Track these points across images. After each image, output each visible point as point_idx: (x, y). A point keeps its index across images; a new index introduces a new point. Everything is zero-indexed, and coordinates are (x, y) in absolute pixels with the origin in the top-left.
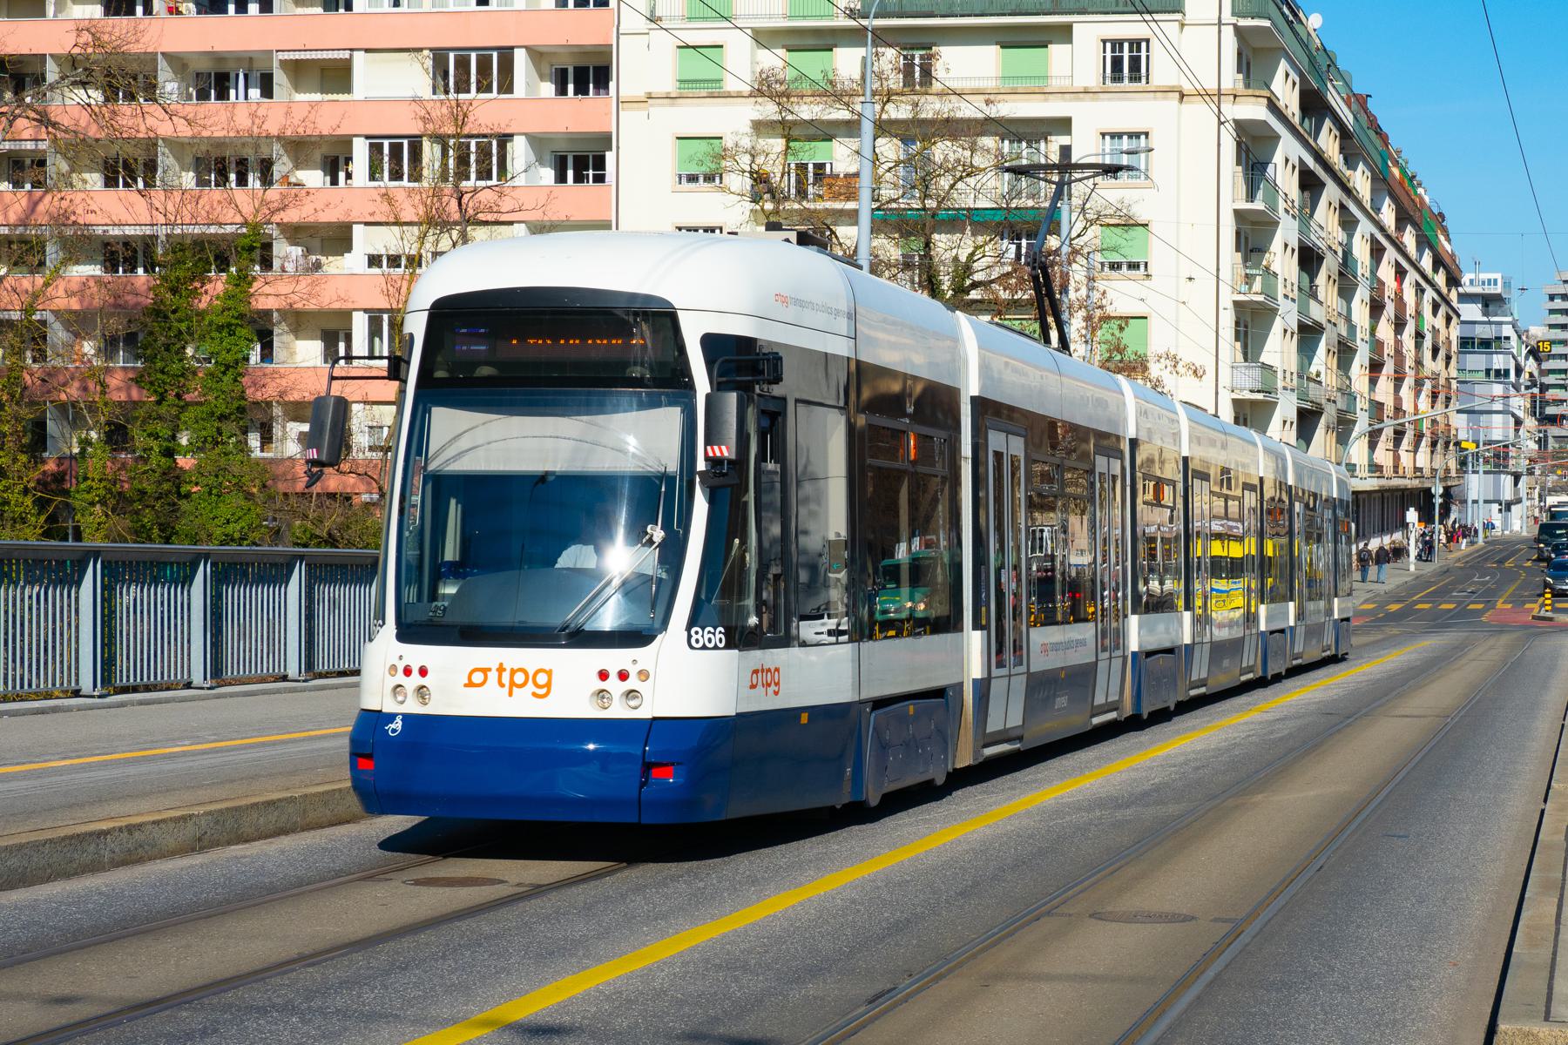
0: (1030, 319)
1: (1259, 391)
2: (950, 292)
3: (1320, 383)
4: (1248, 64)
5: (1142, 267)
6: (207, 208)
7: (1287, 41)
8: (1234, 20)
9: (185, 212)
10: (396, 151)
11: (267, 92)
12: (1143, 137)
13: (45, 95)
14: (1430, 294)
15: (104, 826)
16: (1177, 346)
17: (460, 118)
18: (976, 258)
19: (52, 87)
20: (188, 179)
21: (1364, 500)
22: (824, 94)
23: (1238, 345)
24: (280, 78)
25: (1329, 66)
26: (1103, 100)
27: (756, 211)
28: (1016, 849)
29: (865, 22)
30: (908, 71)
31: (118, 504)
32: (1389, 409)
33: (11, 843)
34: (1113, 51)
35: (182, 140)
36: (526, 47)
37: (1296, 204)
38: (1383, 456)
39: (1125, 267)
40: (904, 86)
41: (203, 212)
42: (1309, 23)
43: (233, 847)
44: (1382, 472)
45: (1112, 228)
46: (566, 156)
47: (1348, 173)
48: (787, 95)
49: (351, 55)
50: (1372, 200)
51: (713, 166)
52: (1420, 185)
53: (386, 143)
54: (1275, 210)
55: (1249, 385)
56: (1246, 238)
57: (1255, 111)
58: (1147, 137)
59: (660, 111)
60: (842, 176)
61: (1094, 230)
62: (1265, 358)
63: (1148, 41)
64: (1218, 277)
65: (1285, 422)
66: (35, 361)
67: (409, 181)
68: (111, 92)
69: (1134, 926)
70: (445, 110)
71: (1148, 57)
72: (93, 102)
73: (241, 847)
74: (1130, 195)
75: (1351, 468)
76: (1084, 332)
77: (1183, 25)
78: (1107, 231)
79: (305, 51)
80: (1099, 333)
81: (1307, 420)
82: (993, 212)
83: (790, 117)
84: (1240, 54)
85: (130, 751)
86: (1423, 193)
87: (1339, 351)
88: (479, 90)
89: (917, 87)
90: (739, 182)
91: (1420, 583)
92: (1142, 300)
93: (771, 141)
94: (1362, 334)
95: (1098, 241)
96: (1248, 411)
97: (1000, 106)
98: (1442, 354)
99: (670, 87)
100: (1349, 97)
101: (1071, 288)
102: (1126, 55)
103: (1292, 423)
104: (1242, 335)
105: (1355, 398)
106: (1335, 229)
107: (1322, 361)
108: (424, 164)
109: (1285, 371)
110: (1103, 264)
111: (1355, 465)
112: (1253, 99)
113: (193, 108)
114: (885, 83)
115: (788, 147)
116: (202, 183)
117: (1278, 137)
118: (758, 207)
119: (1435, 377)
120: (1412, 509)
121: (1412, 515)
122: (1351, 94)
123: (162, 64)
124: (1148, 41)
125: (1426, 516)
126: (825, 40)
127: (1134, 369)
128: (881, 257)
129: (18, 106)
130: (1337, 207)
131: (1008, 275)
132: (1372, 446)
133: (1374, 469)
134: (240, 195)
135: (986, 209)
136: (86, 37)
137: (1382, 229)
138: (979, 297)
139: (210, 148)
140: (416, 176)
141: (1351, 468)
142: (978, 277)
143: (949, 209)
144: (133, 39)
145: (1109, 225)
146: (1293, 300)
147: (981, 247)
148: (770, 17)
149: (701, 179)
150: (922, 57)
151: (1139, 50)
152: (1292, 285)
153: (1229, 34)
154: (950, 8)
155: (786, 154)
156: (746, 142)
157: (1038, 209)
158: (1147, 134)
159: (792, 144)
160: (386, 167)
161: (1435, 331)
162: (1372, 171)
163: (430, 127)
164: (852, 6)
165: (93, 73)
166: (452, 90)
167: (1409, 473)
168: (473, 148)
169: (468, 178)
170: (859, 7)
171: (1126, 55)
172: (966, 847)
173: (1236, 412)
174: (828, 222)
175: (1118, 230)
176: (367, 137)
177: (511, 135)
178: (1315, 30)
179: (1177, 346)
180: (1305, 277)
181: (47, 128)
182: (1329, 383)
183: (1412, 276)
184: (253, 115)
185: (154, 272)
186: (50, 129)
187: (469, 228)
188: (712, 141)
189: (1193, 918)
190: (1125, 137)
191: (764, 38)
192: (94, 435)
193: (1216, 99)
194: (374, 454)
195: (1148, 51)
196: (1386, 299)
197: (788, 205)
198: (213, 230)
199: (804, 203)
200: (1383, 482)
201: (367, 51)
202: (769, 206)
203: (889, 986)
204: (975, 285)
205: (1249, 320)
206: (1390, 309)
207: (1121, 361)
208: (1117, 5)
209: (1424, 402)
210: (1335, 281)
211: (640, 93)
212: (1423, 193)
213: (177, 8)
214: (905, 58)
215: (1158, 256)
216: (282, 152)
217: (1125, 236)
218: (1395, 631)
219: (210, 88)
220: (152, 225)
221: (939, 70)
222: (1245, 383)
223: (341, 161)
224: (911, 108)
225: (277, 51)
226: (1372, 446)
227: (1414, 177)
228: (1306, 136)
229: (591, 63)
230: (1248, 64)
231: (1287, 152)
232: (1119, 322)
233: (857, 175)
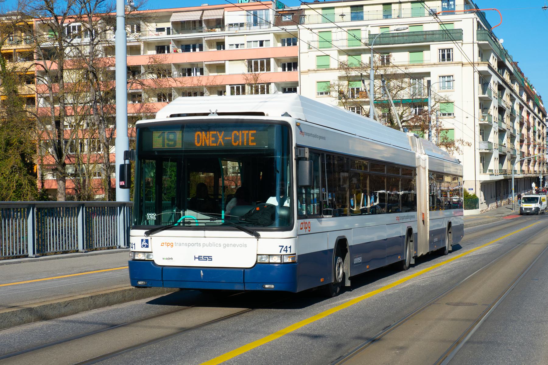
8: (477, 42)
30: (382, 60)
39: (447, 115)
59: (312, 75)
74: (448, 94)
97: (409, 69)
99: (315, 67)
126: (358, 52)
153: (476, 46)
156: (337, 83)
175: (445, 104)
191: (341, 52)
197: (349, 100)
202: (344, 101)
211: (306, 70)
222: (483, 147)
231: (494, 79)
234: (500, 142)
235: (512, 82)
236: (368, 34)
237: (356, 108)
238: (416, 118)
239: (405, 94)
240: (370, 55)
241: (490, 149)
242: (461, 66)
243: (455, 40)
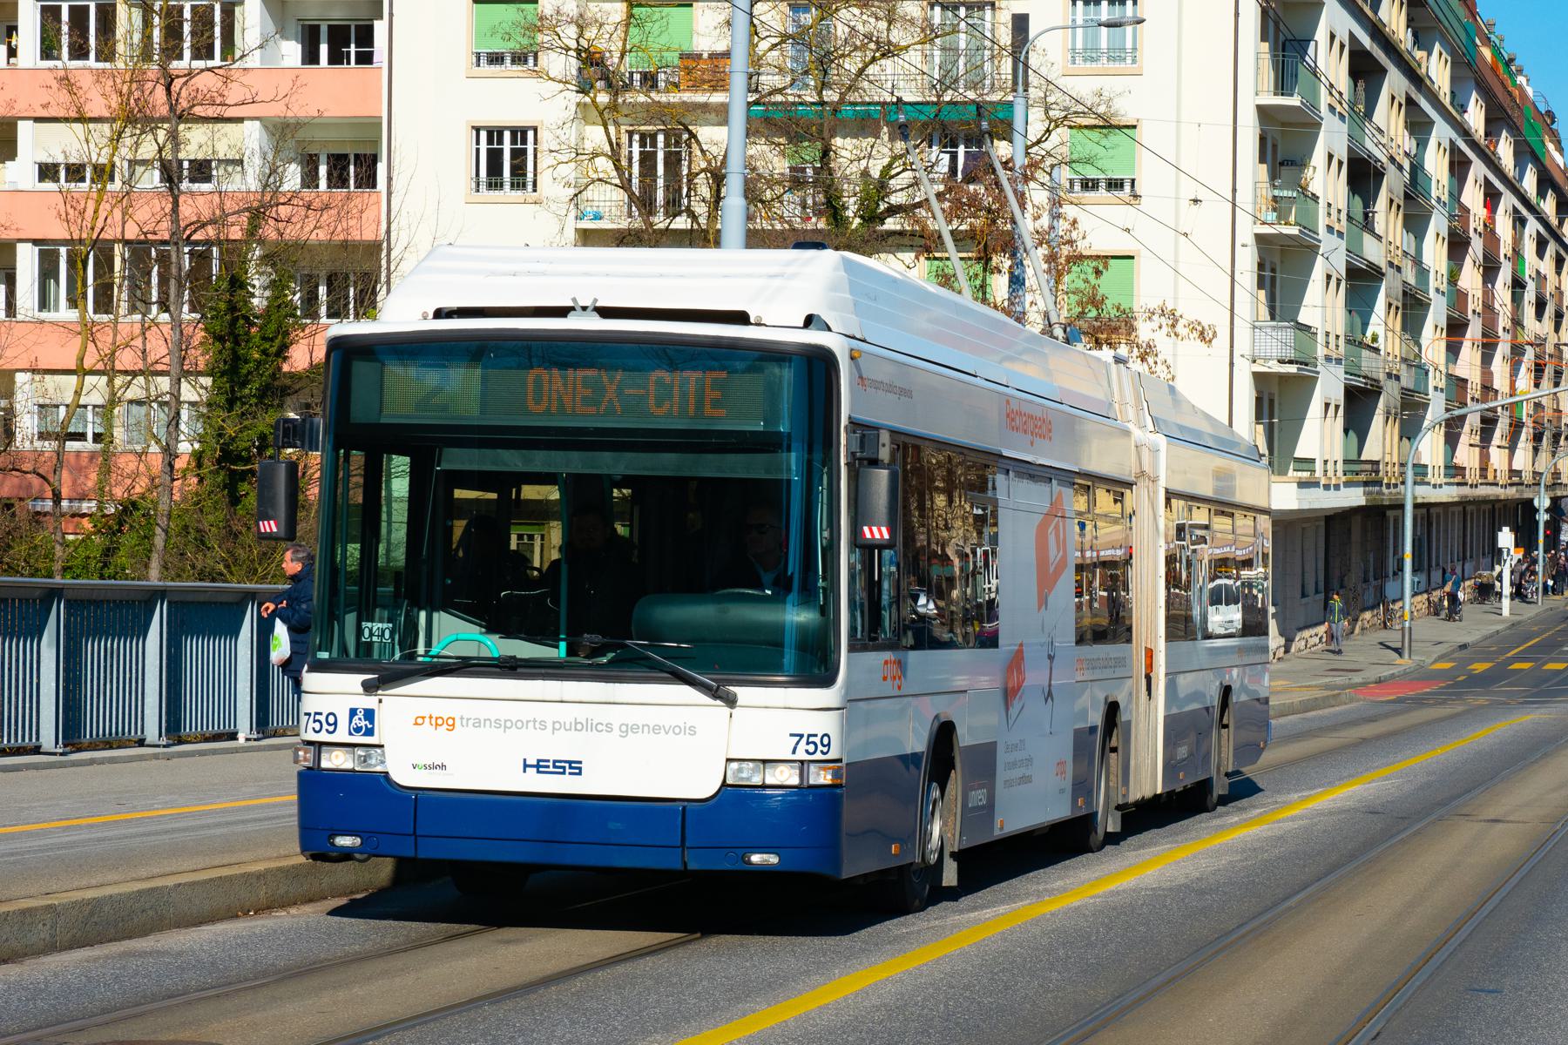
0: (970, 259)
1: (1291, 362)
2: (858, 221)
3: (1377, 350)
5: (1127, 187)
14: (1533, 226)
16: (1176, 298)
18: (893, 172)
21: (1438, 516)
23: (1262, 294)
27: (585, 104)
28: (946, 1006)
32: (1474, 388)
37: (1346, 96)
38: (1466, 455)
44: (1464, 477)
46: (319, 26)
50: (1452, 92)
51: (525, 41)
52: (1520, 71)
54: (1315, 107)
56: (1275, 146)
60: (705, 56)
61: (1060, 134)
62: (1304, 317)
64: (1234, 205)
65: (1327, 405)
67: (97, 60)
74: (1110, 85)
75: (1421, 470)
78: (1079, 135)
80: (1066, 279)
86: (1524, 83)
87: (1405, 306)
90: (560, 64)
91: (1517, 633)
92: (1128, 230)
94: (1437, 281)
95: (1065, 150)
96: (1275, 390)
98: (1550, 310)
103: (1337, 407)
105: (1427, 373)
107: (1382, 322)
108: (118, 36)
109: (1327, 334)
110: (1071, 182)
111: (1426, 466)
115: (631, 16)
118: (587, 100)
119: (1539, 343)
120: (1506, 529)
121: (1506, 538)
125: (1526, 539)
127: (1116, 330)
128: (761, 171)
130: (1403, 102)
132: (1452, 440)
133: (1452, 471)
137: (1465, 132)
138: (898, 227)
140: (106, 54)
141: (1419, 470)
142: (897, 199)
143: (854, 104)
145: (1081, 127)
146: (1340, 234)
147: (901, 156)
149: (508, 60)
152: (1339, 211)
155: (628, 25)
159: (636, 11)
160: (65, 40)
161: (1540, 278)
162: (1453, 53)
167: (1503, 478)
169: (180, 57)
172: (875, 1001)
173: (1258, 391)
174: (686, 121)
175: (1095, 135)
179: (1176, 298)
180: (1358, 200)
182: (1390, 350)
183: (1508, 201)
187: (181, 127)
194: (46, 443)
196: (1472, 233)
197: (629, 97)
199: (653, 95)
200: (1466, 491)
202: (603, 98)
204: (893, 210)
205: (1277, 260)
206: (1477, 246)
207: (1096, 319)
209: (1524, 381)
210: (1399, 207)
212: (1524, 83)
215: (1149, 175)
217: (1105, 141)
218: (1482, 700)
226: (1452, 440)
227: (1512, 60)
232: (1095, 264)
233: (727, 55)
234: (1350, 327)
237: (661, 138)
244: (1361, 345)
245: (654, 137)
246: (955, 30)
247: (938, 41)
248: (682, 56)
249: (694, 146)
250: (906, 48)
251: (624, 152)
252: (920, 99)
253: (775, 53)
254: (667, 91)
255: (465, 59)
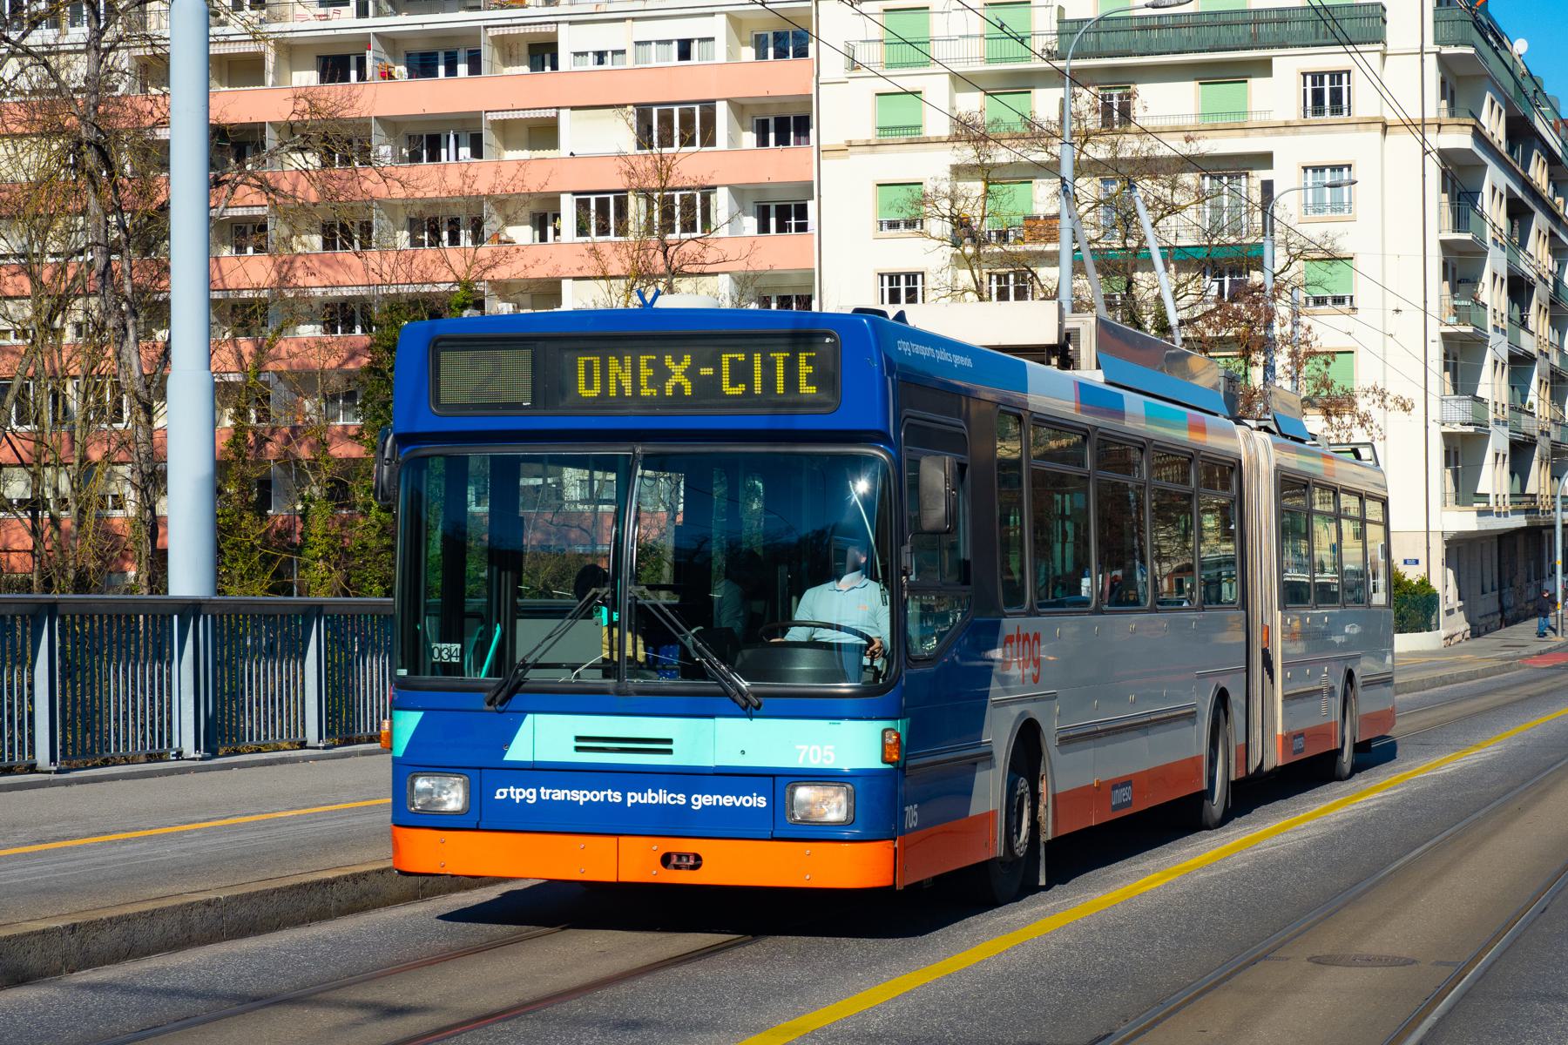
0: (1236, 356)
1: (1469, 424)
2: (1153, 332)
3: (1532, 414)
4: (1452, 92)
6: (421, 267)
7: (1494, 65)
8: (1437, 49)
9: (400, 272)
10: (602, 206)
11: (477, 152)
12: (1346, 170)
13: (265, 162)
15: (330, 875)
16: (1385, 380)
17: (664, 171)
19: (272, 154)
20: (403, 238)
22: (1022, 137)
24: (488, 138)
25: (1535, 91)
26: (1304, 133)
27: (957, 255)
28: (1231, 892)
29: (1059, 64)
30: (1107, 110)
31: (340, 559)
33: (240, 892)
34: (1314, 83)
35: (395, 202)
36: (728, 100)
37: (1505, 232)
39: (1329, 302)
40: (1103, 126)
41: (417, 272)
42: (1515, 50)
43: (454, 895)
45: (1316, 263)
46: (769, 206)
47: (1558, 200)
48: (985, 138)
49: (557, 114)
51: (913, 212)
53: (593, 198)
55: (1459, 417)
57: (1460, 139)
58: (1350, 170)
59: (859, 159)
60: (1042, 218)
61: (1298, 265)
63: (1349, 72)
64: (1426, 312)
65: (1497, 455)
66: (259, 420)
67: (616, 236)
68: (327, 160)
69: (1353, 970)
70: (649, 165)
71: (1349, 88)
72: (310, 167)
73: (461, 895)
74: (1333, 229)
76: (1289, 368)
77: (1384, 56)
79: (513, 110)
80: (1305, 368)
81: (1520, 452)
82: (1194, 250)
83: (987, 161)
84: (1443, 83)
85: (354, 801)
87: (1552, 382)
88: (682, 144)
89: (1116, 127)
90: (939, 227)
92: (1349, 334)
93: (971, 184)
95: (1301, 276)
96: (1459, 445)
97: (1200, 143)
99: (869, 134)
100: (1556, 123)
101: (1276, 324)
102: (1327, 87)
103: (1504, 456)
104: (1451, 368)
106: (1545, 257)
108: (630, 218)
109: (1496, 404)
110: (1307, 299)
112: (1458, 128)
113: (404, 171)
114: (1083, 124)
115: (987, 191)
116: (416, 243)
117: (1485, 166)
118: (958, 252)
122: (1558, 120)
123: (376, 128)
124: (1349, 72)
126: (1023, 82)
127: (1340, 405)
129: (240, 174)
130: (1547, 234)
131: (1212, 312)
134: (453, 254)
135: (1188, 247)
136: (303, 104)
139: (423, 210)
140: (622, 230)
144: (348, 103)
145: (1313, 260)
147: (1184, 285)
148: (969, 60)
149: (902, 225)
150: (1120, 97)
151: (1340, 82)
152: (1502, 315)
153: (1431, 62)
154: (1148, 46)
155: (985, 198)
156: (945, 187)
157: (1240, 245)
158: (1349, 167)
159: (991, 187)
160: (593, 222)
163: (635, 181)
164: (1050, 48)
165: (311, 140)
166: (656, 145)
168: (677, 201)
169: (673, 231)
170: (1056, 48)
171: (1327, 87)
172: (1180, 890)
173: (1446, 446)
174: (1029, 264)
175: (1323, 265)
176: (575, 193)
177: (715, 187)
178: (1520, 56)
179: (1385, 380)
181: (267, 194)
182: (1542, 414)
184: (464, 175)
185: (371, 331)
186: (271, 195)
187: (675, 280)
188: (911, 187)
189: (1414, 962)
190: (1328, 170)
191: (962, 81)
192: (316, 490)
193: (1420, 128)
194: (586, 507)
195: (1349, 83)
197: (988, 249)
198: (426, 289)
199: (1005, 247)
201: (573, 108)
202: (970, 250)
203: (1105, 1032)
205: (1458, 352)
207: (1328, 396)
208: (1317, 37)
210: (1546, 310)
211: (840, 142)
213: (390, 74)
214: (1103, 98)
215: (1363, 293)
216: (492, 210)
219: (422, 150)
220: (369, 285)
221: (1137, 111)
222: (1457, 416)
223: (550, 218)
224: (1109, 147)
225: (486, 112)
228: (1513, 163)
229: (792, 113)
230: (1452, 92)
231: (1494, 178)
232: (1325, 357)
233: (1057, 216)
234: (1513, 398)
235: (1557, 192)
236: (1055, 18)
237: (1012, 277)
238: (1223, 310)
239: (1185, 229)
240: (1057, 93)
241: (1481, 424)
242: (1379, 134)
243: (1351, 43)
244: (1521, 411)
245: (1006, 277)
246: (1220, 194)
247: (1208, 202)
248: (1026, 219)
249: (1035, 282)
250: (1184, 208)
251: (986, 287)
252: (1196, 244)
253: (1091, 214)
254: (1015, 243)
255: (872, 225)
